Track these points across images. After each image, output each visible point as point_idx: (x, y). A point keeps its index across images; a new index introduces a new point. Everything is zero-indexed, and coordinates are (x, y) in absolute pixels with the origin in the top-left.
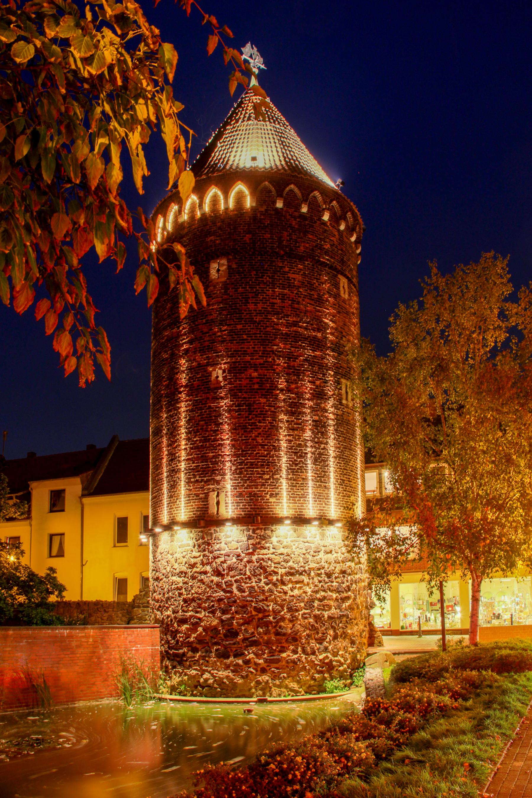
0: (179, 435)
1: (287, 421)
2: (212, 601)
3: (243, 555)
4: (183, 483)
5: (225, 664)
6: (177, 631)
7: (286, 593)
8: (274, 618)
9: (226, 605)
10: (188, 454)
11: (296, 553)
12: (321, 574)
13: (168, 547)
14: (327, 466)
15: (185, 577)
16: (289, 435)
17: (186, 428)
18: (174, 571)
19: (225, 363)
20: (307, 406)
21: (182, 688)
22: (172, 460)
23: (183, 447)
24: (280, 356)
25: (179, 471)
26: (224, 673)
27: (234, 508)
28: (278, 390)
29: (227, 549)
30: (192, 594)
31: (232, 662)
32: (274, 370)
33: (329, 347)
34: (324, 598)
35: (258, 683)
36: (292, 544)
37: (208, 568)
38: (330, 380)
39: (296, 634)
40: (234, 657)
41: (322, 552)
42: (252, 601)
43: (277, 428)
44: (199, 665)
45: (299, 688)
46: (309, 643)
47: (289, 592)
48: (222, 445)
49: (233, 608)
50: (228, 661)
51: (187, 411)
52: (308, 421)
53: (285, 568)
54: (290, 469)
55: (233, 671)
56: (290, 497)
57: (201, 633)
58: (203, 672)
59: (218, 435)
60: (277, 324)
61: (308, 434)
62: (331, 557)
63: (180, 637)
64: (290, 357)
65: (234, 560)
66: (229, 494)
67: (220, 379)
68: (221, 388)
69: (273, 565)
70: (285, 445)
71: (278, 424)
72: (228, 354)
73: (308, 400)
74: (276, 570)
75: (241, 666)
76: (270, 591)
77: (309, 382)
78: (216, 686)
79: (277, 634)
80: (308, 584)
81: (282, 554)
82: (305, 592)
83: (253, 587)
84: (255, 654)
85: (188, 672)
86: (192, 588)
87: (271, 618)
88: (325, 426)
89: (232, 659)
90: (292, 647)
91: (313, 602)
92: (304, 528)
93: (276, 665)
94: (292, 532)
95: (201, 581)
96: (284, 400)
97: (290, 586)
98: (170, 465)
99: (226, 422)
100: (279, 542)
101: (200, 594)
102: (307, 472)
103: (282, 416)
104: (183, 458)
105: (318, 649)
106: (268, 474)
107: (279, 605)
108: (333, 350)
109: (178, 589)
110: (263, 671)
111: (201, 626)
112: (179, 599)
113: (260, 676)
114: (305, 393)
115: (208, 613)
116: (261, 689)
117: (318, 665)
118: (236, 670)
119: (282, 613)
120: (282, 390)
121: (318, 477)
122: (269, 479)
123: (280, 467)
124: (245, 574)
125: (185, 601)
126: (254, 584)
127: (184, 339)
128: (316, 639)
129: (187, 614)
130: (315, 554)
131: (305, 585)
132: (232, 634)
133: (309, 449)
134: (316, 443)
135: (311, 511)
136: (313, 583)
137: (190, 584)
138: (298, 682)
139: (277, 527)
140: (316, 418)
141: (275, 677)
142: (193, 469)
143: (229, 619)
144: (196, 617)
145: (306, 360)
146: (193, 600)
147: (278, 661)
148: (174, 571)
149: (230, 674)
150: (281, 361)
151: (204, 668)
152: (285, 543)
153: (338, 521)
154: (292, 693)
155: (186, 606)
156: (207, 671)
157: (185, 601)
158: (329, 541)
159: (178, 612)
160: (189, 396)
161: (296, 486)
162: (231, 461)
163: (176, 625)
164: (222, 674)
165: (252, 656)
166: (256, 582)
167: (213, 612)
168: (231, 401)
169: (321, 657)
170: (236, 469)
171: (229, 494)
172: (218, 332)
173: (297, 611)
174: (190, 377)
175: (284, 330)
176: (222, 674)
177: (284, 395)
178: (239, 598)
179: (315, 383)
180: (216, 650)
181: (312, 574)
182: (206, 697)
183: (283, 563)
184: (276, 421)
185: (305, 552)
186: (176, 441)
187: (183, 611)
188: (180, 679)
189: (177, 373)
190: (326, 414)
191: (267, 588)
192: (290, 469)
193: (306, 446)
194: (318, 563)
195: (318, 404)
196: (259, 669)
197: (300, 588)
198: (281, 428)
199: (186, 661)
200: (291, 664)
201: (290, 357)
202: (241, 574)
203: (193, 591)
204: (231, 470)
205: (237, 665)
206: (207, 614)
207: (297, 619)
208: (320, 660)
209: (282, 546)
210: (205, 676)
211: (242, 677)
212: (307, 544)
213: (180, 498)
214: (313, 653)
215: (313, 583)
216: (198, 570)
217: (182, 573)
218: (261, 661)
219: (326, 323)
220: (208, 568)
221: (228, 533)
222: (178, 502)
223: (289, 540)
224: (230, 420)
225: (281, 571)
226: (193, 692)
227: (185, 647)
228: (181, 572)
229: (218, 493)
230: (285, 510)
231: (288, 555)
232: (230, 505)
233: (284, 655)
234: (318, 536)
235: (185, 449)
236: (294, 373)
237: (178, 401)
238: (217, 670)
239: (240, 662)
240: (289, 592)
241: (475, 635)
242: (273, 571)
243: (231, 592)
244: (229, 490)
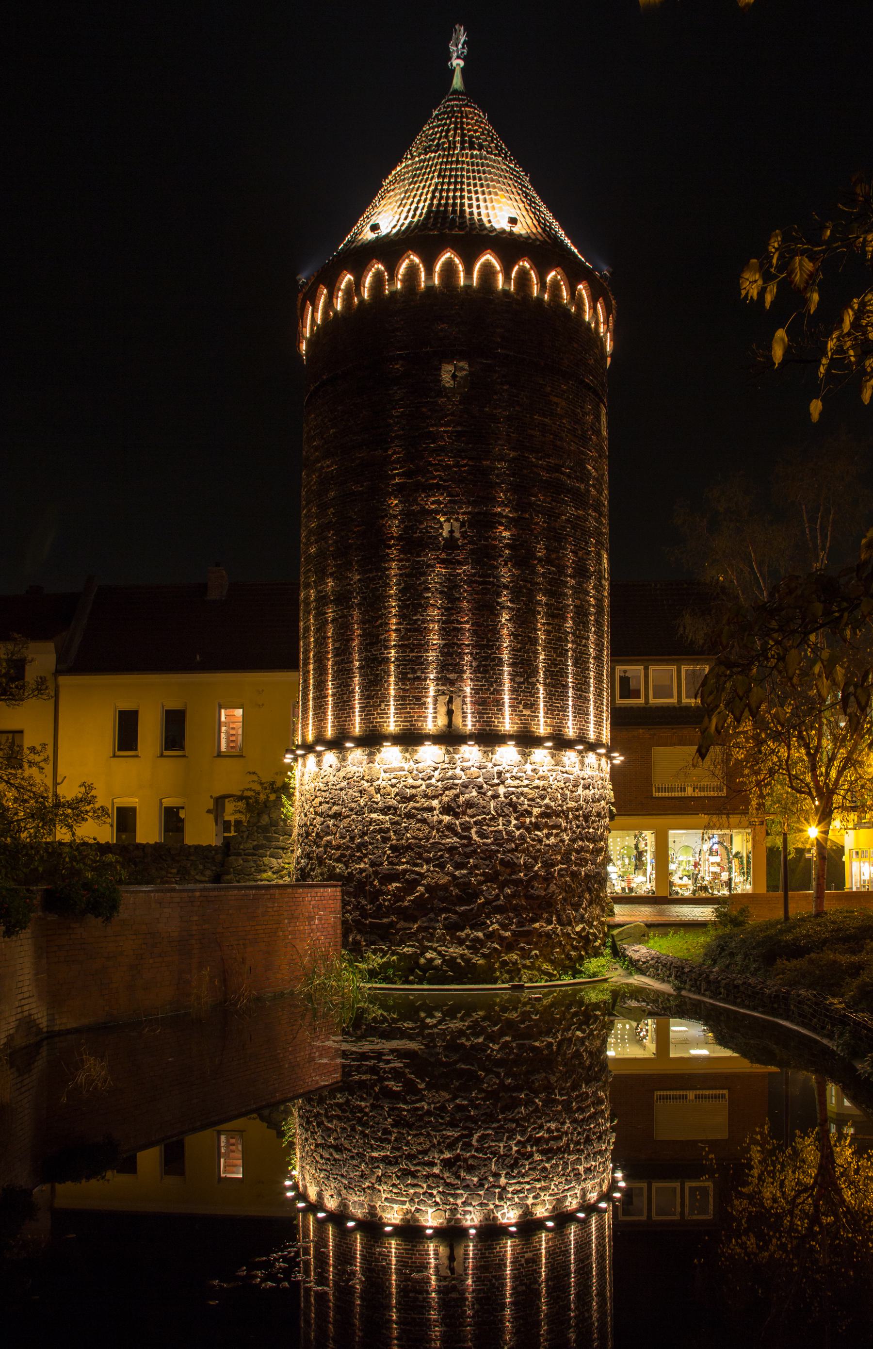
0: (386, 608)
1: (546, 604)
2: (441, 850)
3: (485, 786)
4: (392, 679)
5: (459, 938)
6: (380, 892)
7: (540, 841)
8: (525, 875)
9: (462, 854)
10: (402, 638)
11: (553, 787)
12: (579, 816)
13: (361, 770)
14: (587, 670)
15: (393, 815)
16: (548, 624)
17: (399, 600)
18: (375, 806)
19: (463, 514)
20: (569, 585)
21: (391, 972)
22: (372, 644)
23: (394, 627)
24: (539, 512)
25: (387, 660)
26: (457, 950)
27: (474, 720)
28: (536, 559)
29: (464, 777)
30: (408, 839)
31: (468, 935)
32: (532, 531)
33: (592, 505)
34: (582, 848)
35: (504, 963)
36: (549, 774)
37: (435, 803)
38: (592, 551)
39: (551, 897)
40: (471, 929)
41: (581, 786)
42: (498, 851)
43: (535, 613)
44: (417, 941)
45: (553, 970)
46: (564, 910)
47: (544, 839)
48: (459, 630)
49: (471, 861)
50: (462, 934)
51: (401, 575)
52: (569, 606)
53: (541, 807)
54: (549, 671)
55: (468, 947)
56: (548, 709)
57: (422, 895)
58: (424, 950)
59: (452, 614)
60: (537, 467)
61: (569, 624)
62: (589, 793)
63: (385, 900)
65: (474, 793)
66: (468, 699)
67: (457, 535)
68: (458, 547)
69: (526, 802)
70: (543, 637)
71: (535, 608)
72: (469, 502)
73: (570, 576)
74: (529, 809)
75: (481, 940)
76: (522, 837)
77: (571, 551)
78: (445, 968)
79: (528, 897)
80: (566, 830)
81: (537, 787)
82: (562, 841)
83: (500, 831)
84: (501, 924)
85: (399, 950)
86: (407, 831)
87: (522, 874)
88: (587, 614)
89: (468, 931)
90: (545, 915)
91: (571, 854)
92: (563, 753)
93: (524, 939)
94: (549, 758)
95: (424, 821)
96: (543, 574)
97: (545, 831)
98: (366, 650)
99: (464, 598)
100: (534, 770)
101: (421, 840)
102: (568, 677)
103: (541, 597)
104: (393, 643)
105: (574, 918)
106: (521, 676)
107: (531, 857)
108: (595, 511)
109: (381, 831)
110: (510, 947)
111: (423, 885)
112: (383, 845)
113: (506, 954)
114: (568, 566)
115: (434, 866)
116: (508, 972)
117: (574, 939)
118: (476, 945)
119: (536, 868)
120: (540, 560)
121: (579, 684)
122: (523, 683)
123: (537, 666)
124: (489, 813)
125: (393, 848)
126: (500, 827)
127: (396, 469)
128: (572, 905)
129: (397, 867)
130: (574, 789)
131: (562, 831)
132: (469, 893)
133: (570, 645)
134: (577, 637)
135: (571, 730)
136: (571, 829)
137: (403, 825)
138: (552, 962)
139: (533, 750)
140: (578, 602)
141: (525, 954)
142: (410, 660)
143: (464, 876)
144: (413, 872)
145: (568, 521)
146: (409, 847)
147: (529, 933)
148: (375, 806)
149: (466, 951)
150: (540, 519)
151: (426, 943)
152: (541, 773)
153: (547, 739)
154: (546, 977)
155: (397, 857)
156: (431, 948)
157: (393, 848)
158: (588, 772)
159: (382, 864)
160: (405, 554)
161: (554, 695)
162: (471, 654)
163: (376, 882)
164: (455, 951)
165: (496, 926)
166: (504, 825)
167: (442, 866)
168: (472, 568)
169: (578, 929)
170: (478, 666)
171: (468, 699)
172: (454, 466)
173: (553, 865)
174: (406, 526)
176: (455, 951)
177: (543, 567)
178: (479, 847)
179: (577, 553)
180: (445, 919)
181: (571, 816)
182: (429, 983)
183: (538, 800)
184: (532, 603)
185: (563, 786)
186: (380, 617)
187: (390, 863)
188: (385, 960)
189: (383, 518)
190: (588, 598)
191: (518, 833)
192: (549, 671)
193: (568, 641)
194: (577, 802)
195: (580, 584)
196: (505, 944)
197: (557, 835)
198: (539, 613)
199: (397, 933)
200: (544, 939)
202: (484, 813)
203: (409, 835)
204: (471, 666)
205: (477, 940)
206: (432, 869)
207: (553, 877)
208: (577, 933)
209: (537, 776)
210: (428, 955)
211: (484, 956)
212: (565, 775)
213: (389, 701)
214: (570, 924)
215: (571, 829)
216: (418, 805)
217: (386, 810)
218: (508, 934)
219: (589, 471)
220: (435, 803)
221: (466, 756)
222: (383, 707)
223: (545, 768)
224: (471, 595)
225: (536, 811)
226: (407, 977)
227: (393, 914)
228: (389, 808)
229: (451, 698)
230: (542, 727)
231: (545, 790)
232: (469, 716)
233: (537, 925)
234: (577, 765)
235: (396, 630)
236: (555, 538)
237: (386, 558)
238: (446, 946)
239: (480, 934)
240: (544, 839)
241: (822, 902)
242: (526, 810)
243: (470, 838)
244: (469, 695)
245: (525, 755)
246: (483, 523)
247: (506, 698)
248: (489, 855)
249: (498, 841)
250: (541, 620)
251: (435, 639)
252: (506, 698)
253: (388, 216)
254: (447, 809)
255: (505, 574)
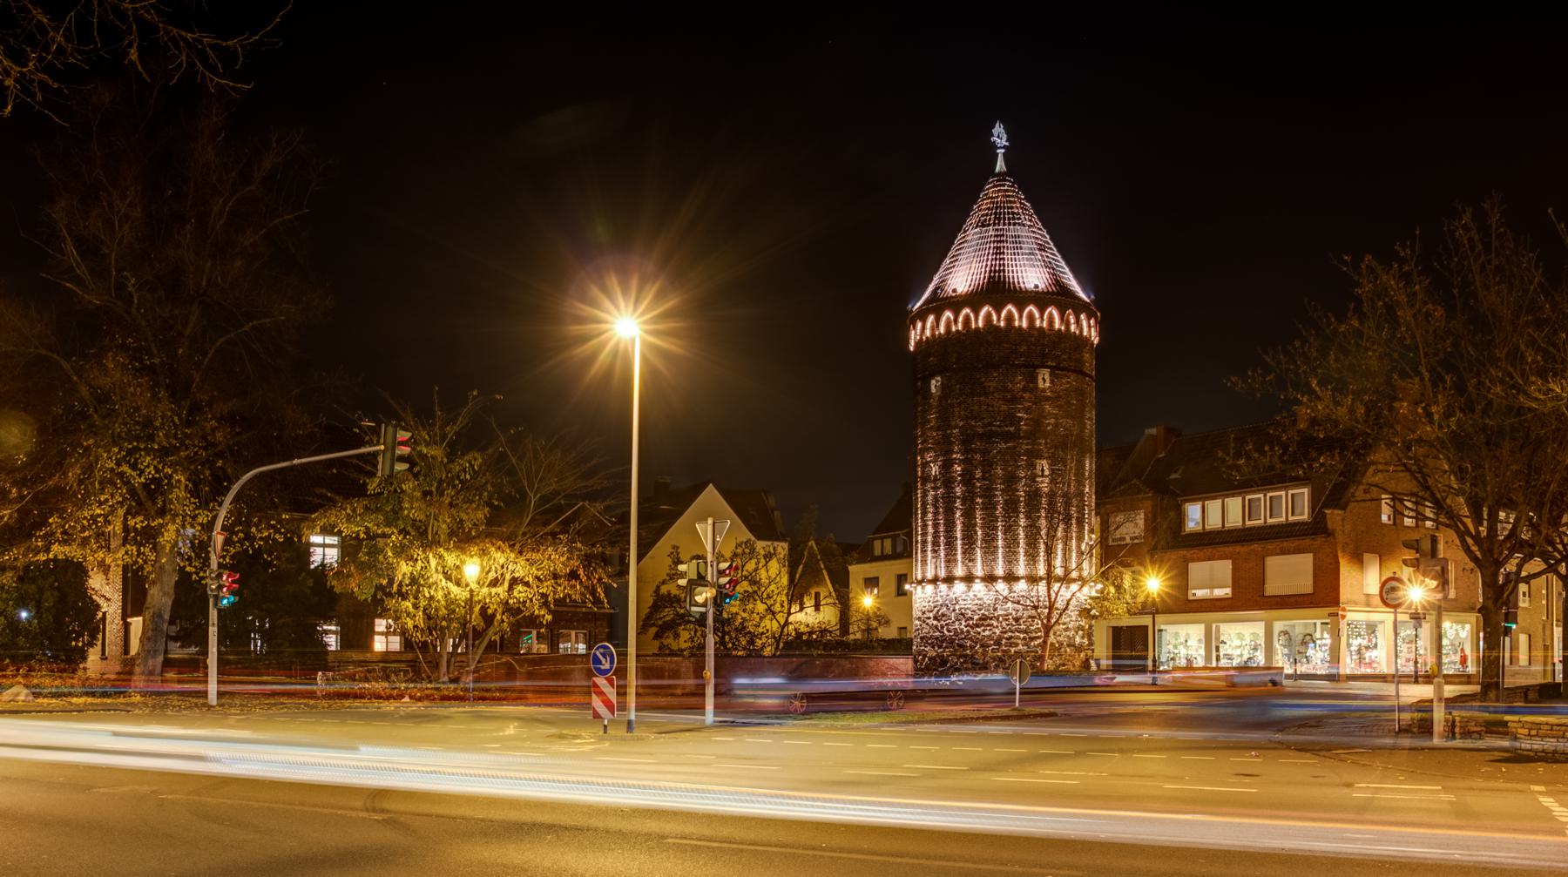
9: (940, 642)
43: (974, 510)
64: (985, 452)
103: (979, 500)
132: (944, 662)
150: (978, 457)
175: (980, 430)
201: (985, 452)
245: (969, 588)
246: (947, 466)
247: (959, 557)
248: (952, 641)
249: (956, 634)
250: (978, 514)
251: (930, 530)
252: (959, 557)
253: (962, 276)
254: (935, 618)
255: (958, 490)
